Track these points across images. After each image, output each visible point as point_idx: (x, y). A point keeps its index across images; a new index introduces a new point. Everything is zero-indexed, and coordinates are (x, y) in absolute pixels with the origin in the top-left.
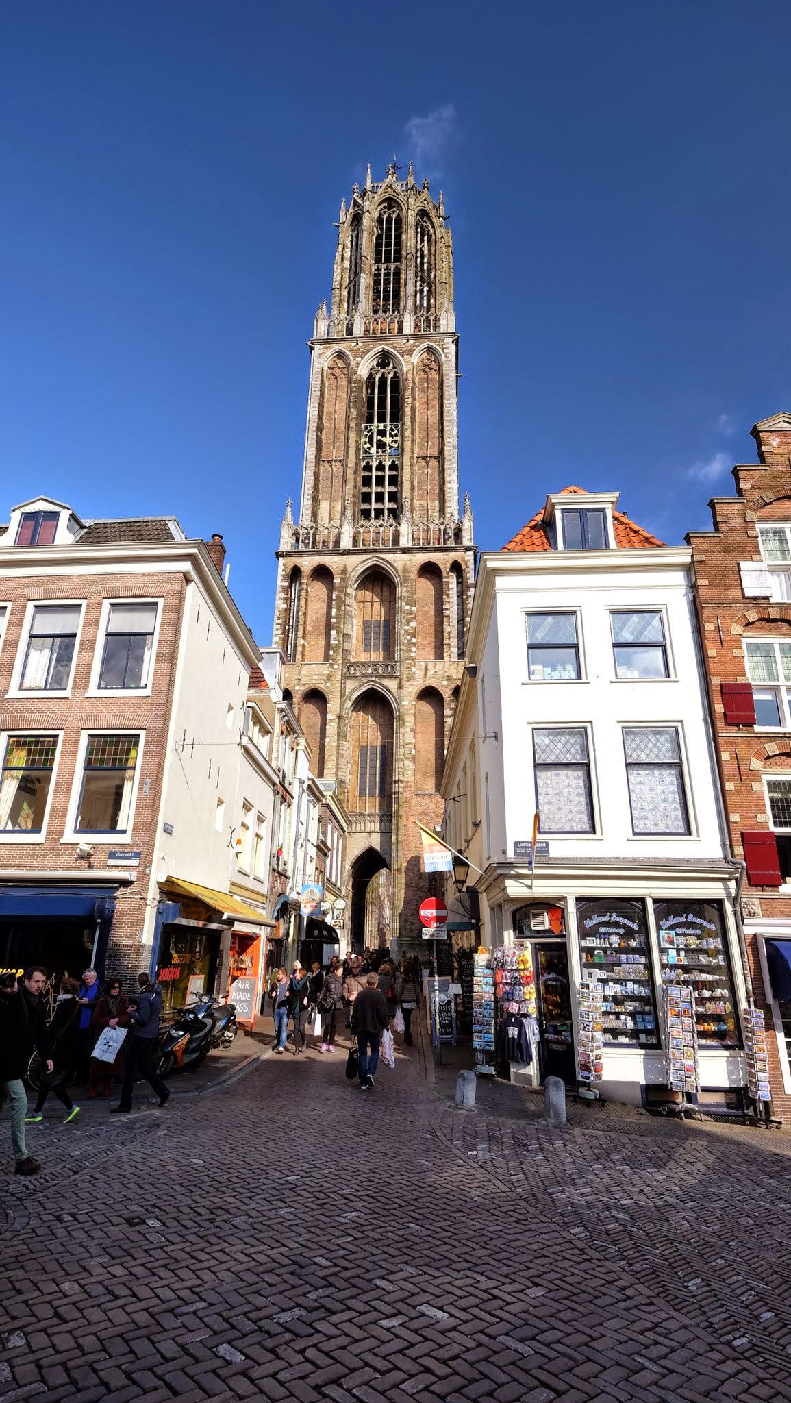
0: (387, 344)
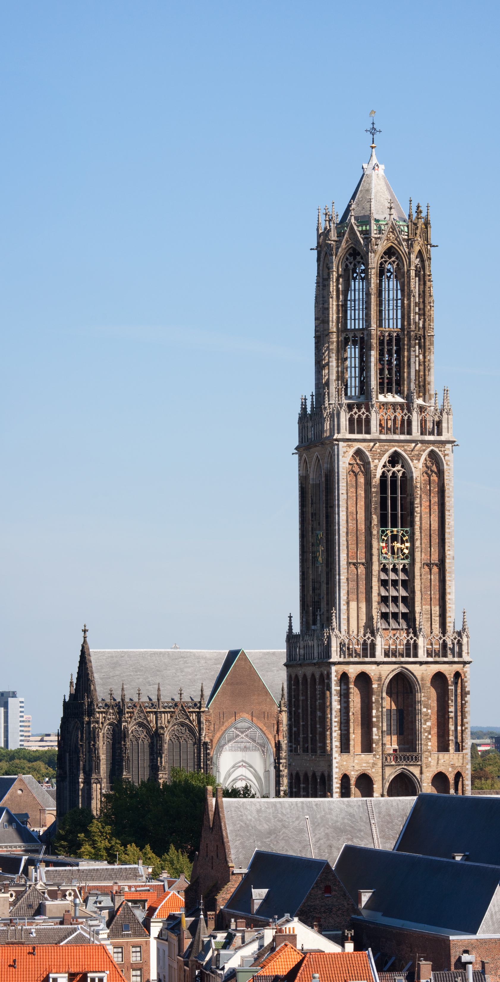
0: (399, 446)
